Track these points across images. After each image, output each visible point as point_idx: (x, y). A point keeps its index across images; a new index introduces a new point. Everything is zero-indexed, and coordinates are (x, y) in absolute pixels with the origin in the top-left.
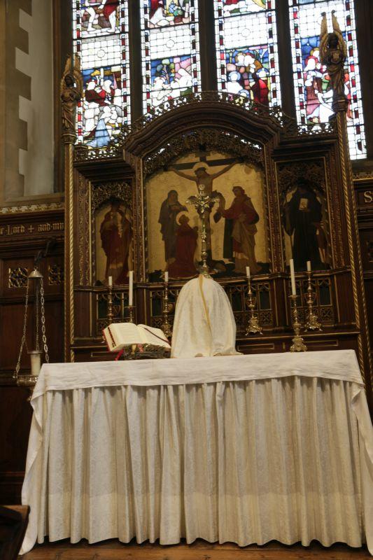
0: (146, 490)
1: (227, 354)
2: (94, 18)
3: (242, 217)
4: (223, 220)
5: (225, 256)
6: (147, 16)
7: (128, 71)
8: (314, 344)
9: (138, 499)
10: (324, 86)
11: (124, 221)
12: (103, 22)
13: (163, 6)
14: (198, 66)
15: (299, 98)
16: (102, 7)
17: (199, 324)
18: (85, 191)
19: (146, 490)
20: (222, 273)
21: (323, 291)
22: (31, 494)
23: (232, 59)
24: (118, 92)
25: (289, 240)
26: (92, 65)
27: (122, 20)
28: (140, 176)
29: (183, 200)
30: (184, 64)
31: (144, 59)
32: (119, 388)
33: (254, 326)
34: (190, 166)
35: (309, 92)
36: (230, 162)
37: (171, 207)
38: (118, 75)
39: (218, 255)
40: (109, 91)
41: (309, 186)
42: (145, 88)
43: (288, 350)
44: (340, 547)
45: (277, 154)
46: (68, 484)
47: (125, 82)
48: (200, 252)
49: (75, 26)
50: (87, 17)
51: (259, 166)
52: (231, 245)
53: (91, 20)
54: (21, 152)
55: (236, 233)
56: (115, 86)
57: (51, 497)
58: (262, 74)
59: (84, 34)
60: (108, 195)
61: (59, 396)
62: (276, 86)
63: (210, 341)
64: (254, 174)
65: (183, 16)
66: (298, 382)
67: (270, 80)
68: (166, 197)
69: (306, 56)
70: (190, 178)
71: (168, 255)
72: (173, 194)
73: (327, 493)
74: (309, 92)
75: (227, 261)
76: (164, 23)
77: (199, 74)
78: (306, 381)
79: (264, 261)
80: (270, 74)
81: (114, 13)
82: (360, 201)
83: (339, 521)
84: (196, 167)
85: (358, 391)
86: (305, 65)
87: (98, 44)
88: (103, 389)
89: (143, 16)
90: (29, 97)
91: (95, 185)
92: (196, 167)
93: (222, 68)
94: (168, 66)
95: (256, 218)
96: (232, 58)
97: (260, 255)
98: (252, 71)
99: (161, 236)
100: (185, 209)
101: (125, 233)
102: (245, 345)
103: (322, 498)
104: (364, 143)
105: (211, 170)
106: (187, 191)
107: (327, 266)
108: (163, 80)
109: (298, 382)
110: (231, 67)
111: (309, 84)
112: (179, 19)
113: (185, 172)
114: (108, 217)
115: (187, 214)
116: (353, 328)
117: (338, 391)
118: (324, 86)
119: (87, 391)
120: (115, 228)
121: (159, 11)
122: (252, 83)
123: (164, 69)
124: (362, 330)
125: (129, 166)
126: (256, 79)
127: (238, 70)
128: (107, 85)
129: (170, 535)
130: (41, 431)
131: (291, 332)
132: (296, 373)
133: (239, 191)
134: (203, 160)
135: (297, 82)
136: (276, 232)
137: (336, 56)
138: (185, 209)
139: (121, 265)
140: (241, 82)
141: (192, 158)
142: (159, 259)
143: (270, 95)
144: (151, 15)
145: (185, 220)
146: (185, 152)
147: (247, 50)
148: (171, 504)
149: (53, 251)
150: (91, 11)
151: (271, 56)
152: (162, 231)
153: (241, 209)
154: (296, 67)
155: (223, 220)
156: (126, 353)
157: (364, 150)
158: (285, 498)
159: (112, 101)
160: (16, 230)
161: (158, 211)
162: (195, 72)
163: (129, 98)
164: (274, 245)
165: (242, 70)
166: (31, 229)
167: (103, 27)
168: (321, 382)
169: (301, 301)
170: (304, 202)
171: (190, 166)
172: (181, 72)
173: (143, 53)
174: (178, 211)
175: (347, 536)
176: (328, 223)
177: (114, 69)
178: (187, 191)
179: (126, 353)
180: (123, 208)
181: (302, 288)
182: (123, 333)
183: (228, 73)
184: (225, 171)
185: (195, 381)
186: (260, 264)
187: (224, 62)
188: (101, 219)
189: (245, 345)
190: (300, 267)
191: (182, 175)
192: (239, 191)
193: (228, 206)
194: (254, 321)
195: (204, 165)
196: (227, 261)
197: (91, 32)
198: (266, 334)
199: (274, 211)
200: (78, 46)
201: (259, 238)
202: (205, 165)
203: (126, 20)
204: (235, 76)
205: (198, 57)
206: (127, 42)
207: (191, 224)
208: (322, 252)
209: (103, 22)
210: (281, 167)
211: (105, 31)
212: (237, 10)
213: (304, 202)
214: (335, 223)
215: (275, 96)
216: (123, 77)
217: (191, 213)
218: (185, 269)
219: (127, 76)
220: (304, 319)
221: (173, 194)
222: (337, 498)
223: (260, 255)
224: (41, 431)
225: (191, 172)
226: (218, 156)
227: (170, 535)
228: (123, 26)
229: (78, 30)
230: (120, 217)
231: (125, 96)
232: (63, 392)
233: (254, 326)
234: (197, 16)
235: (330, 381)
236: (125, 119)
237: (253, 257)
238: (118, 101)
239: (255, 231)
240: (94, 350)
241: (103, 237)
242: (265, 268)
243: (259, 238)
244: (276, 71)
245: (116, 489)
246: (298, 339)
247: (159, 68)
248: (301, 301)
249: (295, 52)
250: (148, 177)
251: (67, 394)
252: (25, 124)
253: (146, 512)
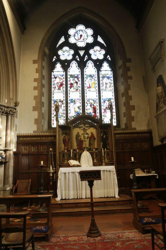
0: (79, 190)
1: (91, 166)
2: (57, 88)
3: (92, 138)
4: (88, 139)
5: (89, 146)
6: (70, 89)
7: (65, 101)
8: (107, 164)
9: (78, 191)
10: (108, 109)
11: (68, 138)
12: (59, 89)
13: (73, 87)
14: (81, 101)
15: (103, 111)
16: (59, 85)
17: (86, 161)
18: (60, 132)
19: (79, 190)
20: (89, 150)
21: (108, 154)
22: (58, 192)
23: (89, 101)
24: (62, 105)
25: (102, 144)
26: (56, 99)
27: (64, 89)
28: (72, 129)
29: (80, 134)
30: (78, 100)
31: (69, 99)
32: (75, 172)
33: (95, 161)
34: (82, 127)
35: (105, 110)
36: (90, 127)
37: (78, 136)
38: (62, 101)
39: (88, 146)
40: (60, 105)
41: (105, 133)
42: (69, 105)
43: (102, 165)
44: (112, 197)
45: (100, 127)
46: (65, 189)
47: (64, 103)
48: (84, 146)
49: (52, 89)
50: (55, 87)
51: (96, 128)
52: (90, 144)
53: (56, 88)
54: (43, 120)
55: (91, 141)
56: (62, 104)
57: (63, 191)
58: (95, 105)
59: (54, 91)
60: (65, 132)
61: (63, 174)
62: (98, 108)
63: (89, 164)
64: (95, 130)
65: (78, 90)
66: (105, 171)
67: (97, 106)
68: (77, 133)
69: (104, 102)
70: (82, 130)
71: (77, 145)
72: (78, 133)
73: (109, 189)
74: (105, 110)
75: (89, 147)
76: (73, 90)
77: (81, 103)
78: (107, 171)
79: (97, 148)
80: (97, 105)
81: (62, 87)
82: (115, 137)
83: (111, 193)
84: (83, 127)
85: (115, 172)
86: (104, 104)
87: (58, 93)
88: (71, 172)
89: (69, 89)
90: (44, 107)
91: (62, 130)
92: (83, 127)
93: (86, 102)
94: (74, 101)
95: (95, 139)
96: (89, 101)
97: (96, 147)
98: (93, 104)
99: (76, 142)
100: (81, 136)
101: (68, 141)
102: (94, 165)
103: (109, 190)
104: (116, 122)
105: (86, 128)
106: (81, 132)
107: (109, 149)
108: (73, 103)
109: (105, 171)
110: (88, 103)
111: (105, 108)
112: (77, 90)
113: (81, 128)
114: (64, 137)
115: (81, 137)
116: (113, 162)
117: (112, 172)
118: (108, 109)
119: (69, 173)
120: (66, 139)
121: (72, 88)
122: (93, 106)
123: (73, 101)
124: (115, 162)
125: (70, 127)
126: (94, 106)
127: (90, 103)
128: (60, 103)
129: (84, 197)
130: (60, 180)
131: (102, 162)
132: (105, 169)
133: (92, 133)
134: (85, 126)
135: (102, 107)
136: (99, 142)
137: (111, 109)
138: (81, 136)
139: (67, 147)
140: (91, 106)
141: (82, 125)
142: (75, 146)
143: (97, 110)
144: (71, 88)
145: (81, 138)
146: (81, 124)
147: (92, 99)
148: (84, 192)
149: (53, 144)
150: (56, 86)
151: (97, 101)
152: (76, 140)
153: (92, 138)
154: (102, 104)
155: (88, 139)
156: (74, 166)
157: (116, 123)
158: (103, 190)
159: (61, 107)
160: (43, 138)
161: (75, 136)
162: (80, 103)
163: (65, 107)
164: (98, 145)
165: (91, 103)
166: (47, 138)
167: (59, 90)
168: (109, 171)
169: (104, 156)
170: (105, 136)
171: (82, 127)
172: (77, 102)
173: (68, 97)
174: (79, 137)
175: (112, 195)
176: (109, 141)
177: (62, 100)
178: (81, 132)
179: (74, 166)
180: (68, 135)
181: (104, 154)
182: (73, 162)
183: (88, 104)
184: (89, 129)
185: (103, 170)
186: (96, 148)
187: (87, 101)
188: (63, 137)
189: (94, 165)
190: (104, 149)
191: (80, 129)
192: (92, 133)
193: (90, 136)
194: (95, 160)
195: (85, 127)
196: (89, 147)
197: (56, 91)
198: (97, 162)
199: (99, 138)
200: (53, 94)
201: (96, 143)
202: (85, 127)
203: (65, 89)
204: (89, 105)
205: (81, 100)
206: (65, 94)
207: (82, 139)
208: (108, 146)
209: (59, 89)
210: (100, 129)
211: (60, 91)
212: (90, 90)
213: (105, 136)
214: (111, 141)
215: (98, 110)
216: (64, 102)
217: (82, 137)
218: (82, 149)
219: (64, 102)
220: (105, 160)
221: (78, 133)
222: (111, 190)
223: (96, 147)
224: (60, 179)
225: (82, 128)
226: (88, 125)
227: (84, 197)
228: (64, 90)
229: (53, 90)
230: (67, 137)
231: (64, 107)
232: (64, 173)
233: (95, 161)
234: (81, 90)
235: (110, 171)
236: (64, 112)
237: (95, 147)
238: (62, 107)
239: (95, 141)
240: (68, 166)
241: (63, 141)
242: (97, 149)
243: (96, 143)
244: (98, 104)
245: (74, 190)
246: (104, 164)
247: (72, 101)
248: (104, 156)
249: (102, 101)
250: (73, 129)
251: (65, 173)
252: (43, 113)
253: (80, 194)
